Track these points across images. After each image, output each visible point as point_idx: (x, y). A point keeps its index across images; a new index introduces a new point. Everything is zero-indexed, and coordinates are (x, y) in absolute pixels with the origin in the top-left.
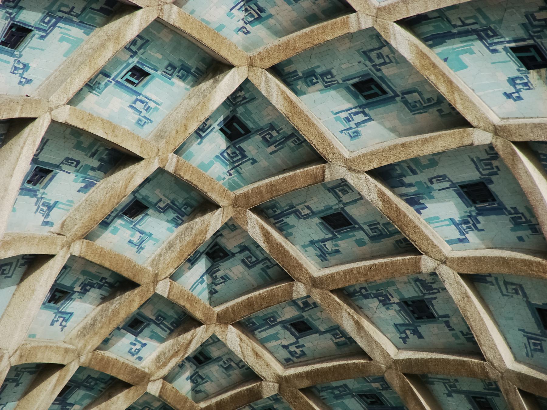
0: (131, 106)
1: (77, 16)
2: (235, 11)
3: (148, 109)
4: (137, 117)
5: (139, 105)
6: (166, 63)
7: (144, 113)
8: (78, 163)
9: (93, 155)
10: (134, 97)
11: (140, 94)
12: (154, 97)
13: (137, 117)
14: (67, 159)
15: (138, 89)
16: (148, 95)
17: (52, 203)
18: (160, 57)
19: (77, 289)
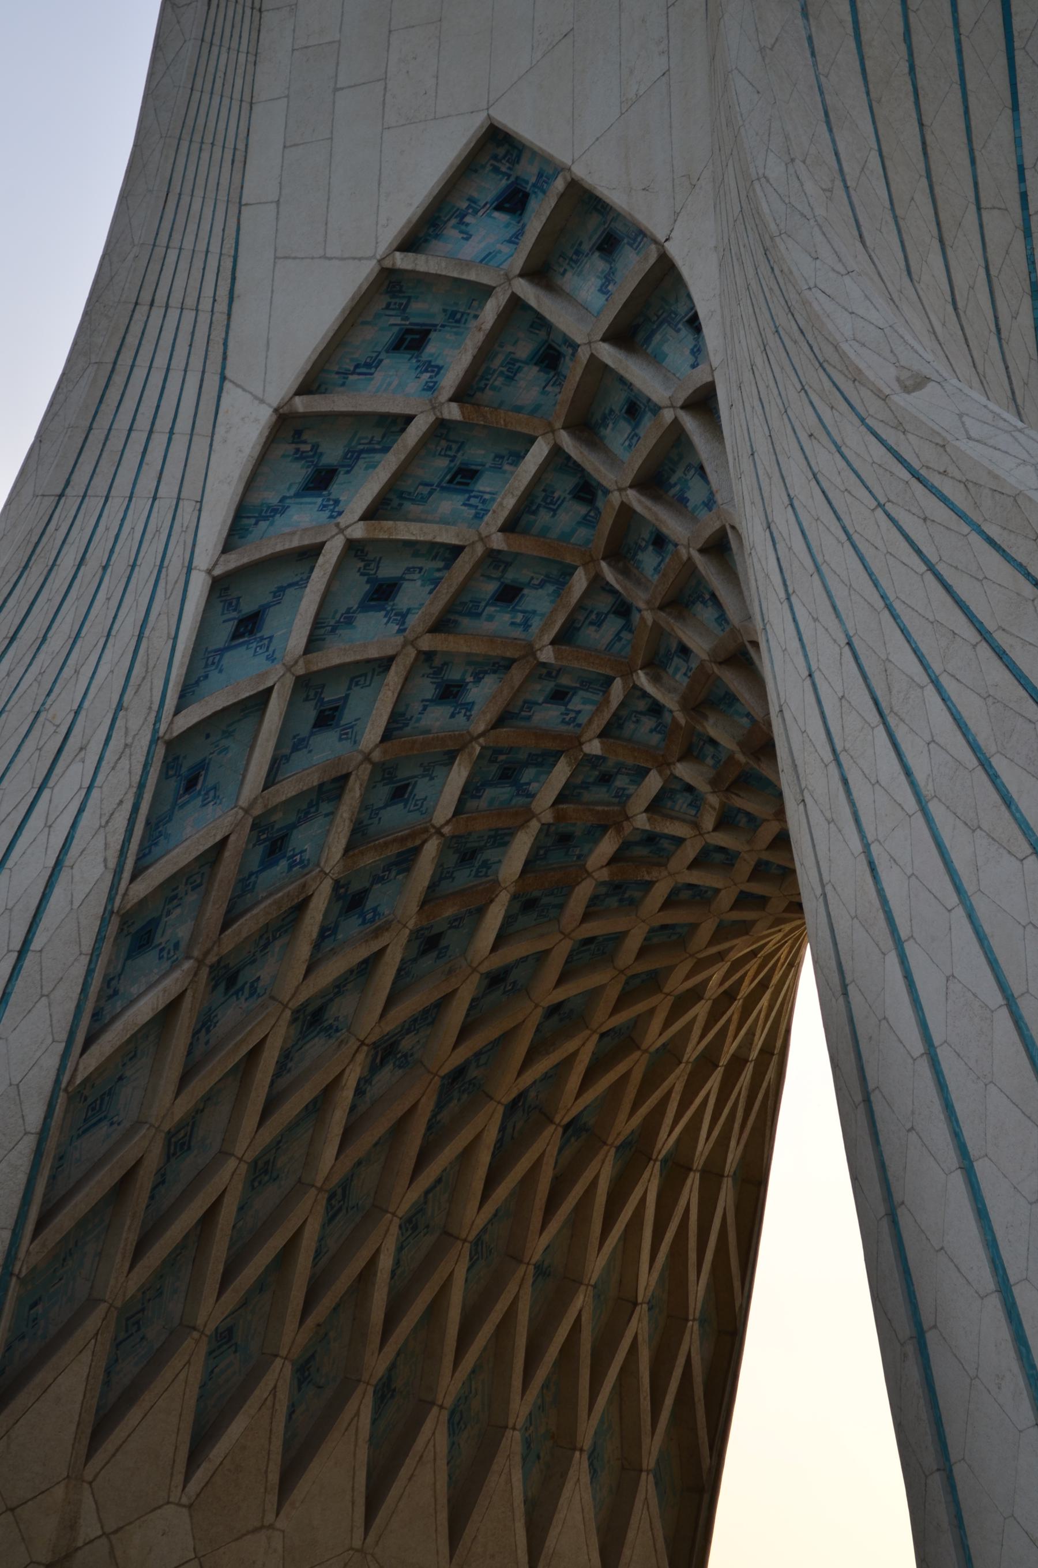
0: (464, 505)
1: (379, 443)
2: (549, 389)
3: (484, 502)
4: (473, 511)
5: (473, 501)
6: (492, 455)
7: (480, 506)
8: (421, 569)
9: (434, 558)
10: (467, 496)
11: (472, 491)
12: (488, 489)
13: (473, 511)
14: (408, 569)
15: (470, 488)
16: (482, 489)
17: (405, 610)
18: (483, 452)
19: (469, 679)
